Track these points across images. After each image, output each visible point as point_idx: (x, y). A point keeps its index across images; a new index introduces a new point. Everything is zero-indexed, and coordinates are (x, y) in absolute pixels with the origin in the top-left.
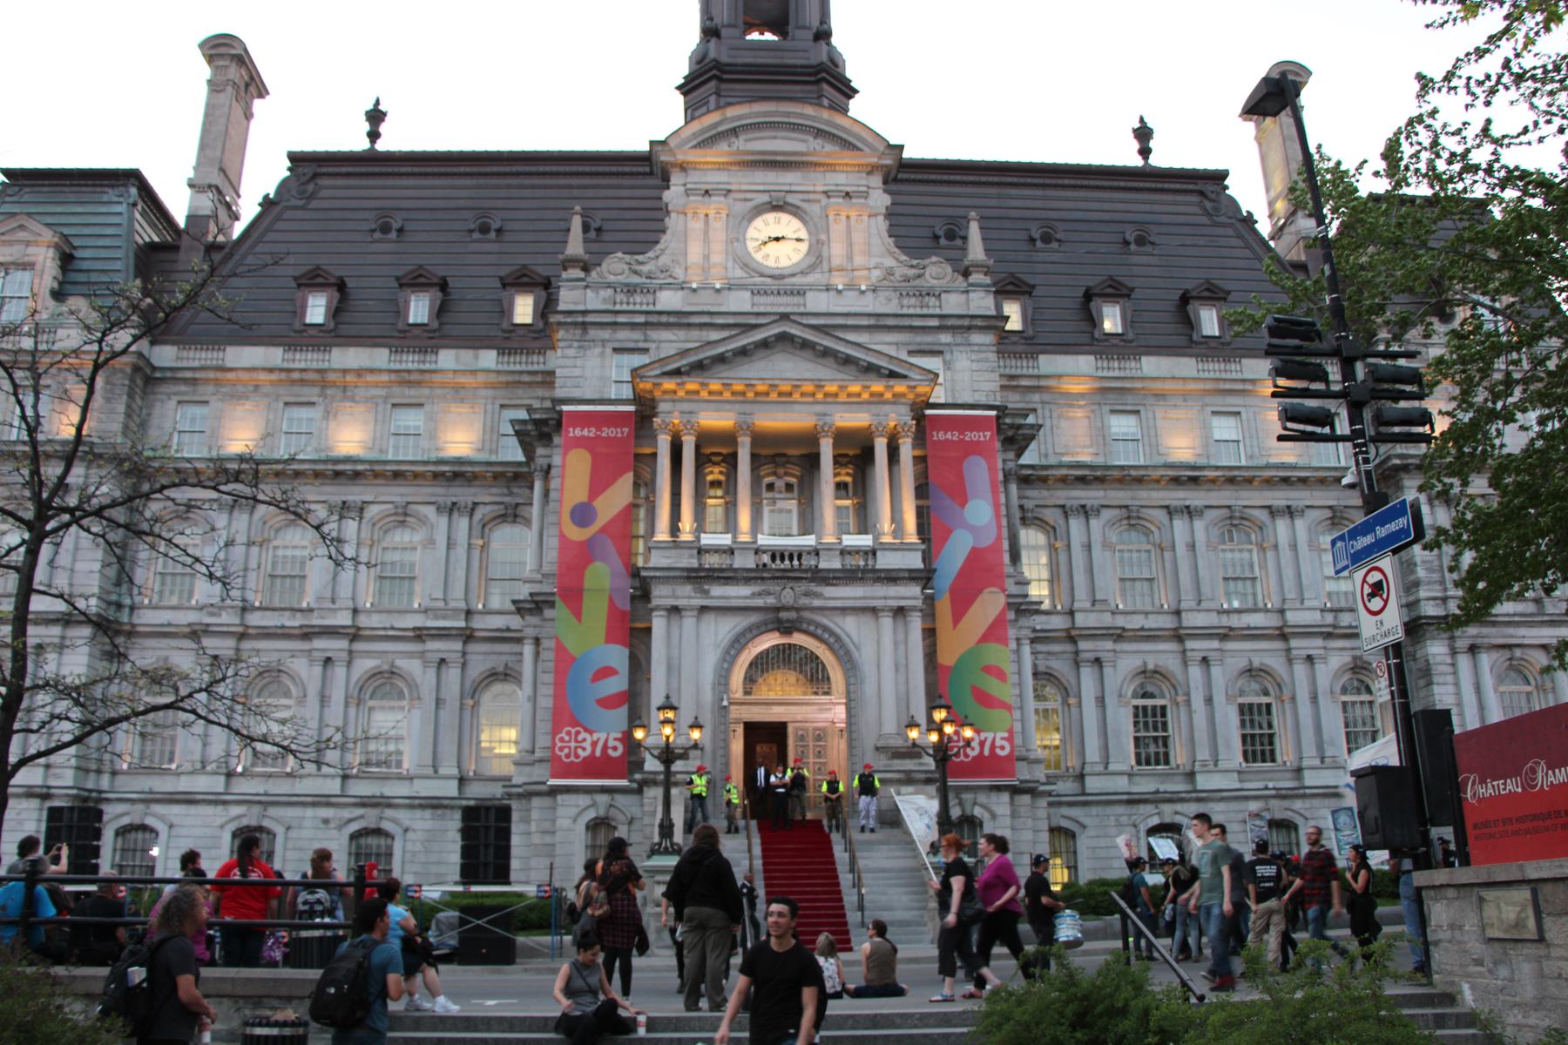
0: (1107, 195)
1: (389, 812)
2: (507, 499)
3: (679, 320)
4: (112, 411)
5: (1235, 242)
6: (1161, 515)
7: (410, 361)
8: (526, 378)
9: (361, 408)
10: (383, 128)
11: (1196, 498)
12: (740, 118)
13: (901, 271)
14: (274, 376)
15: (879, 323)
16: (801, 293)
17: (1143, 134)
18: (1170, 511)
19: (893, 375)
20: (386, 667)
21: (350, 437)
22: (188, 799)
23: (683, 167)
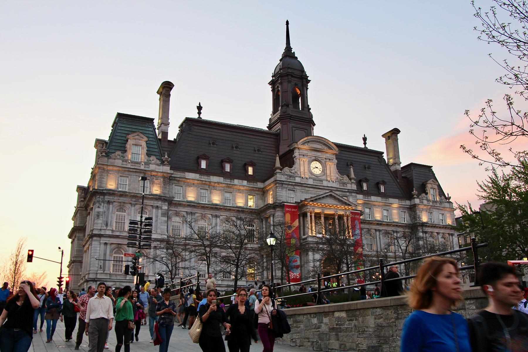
0: (361, 155)
3: (301, 185)
4: (166, 188)
5: (385, 170)
6: (374, 231)
7: (228, 181)
9: (218, 192)
10: (202, 111)
11: (381, 228)
13: (339, 177)
14: (199, 182)
15: (337, 189)
16: (322, 181)
17: (365, 139)
18: (376, 230)
19: (349, 205)
21: (216, 199)
23: (299, 148)
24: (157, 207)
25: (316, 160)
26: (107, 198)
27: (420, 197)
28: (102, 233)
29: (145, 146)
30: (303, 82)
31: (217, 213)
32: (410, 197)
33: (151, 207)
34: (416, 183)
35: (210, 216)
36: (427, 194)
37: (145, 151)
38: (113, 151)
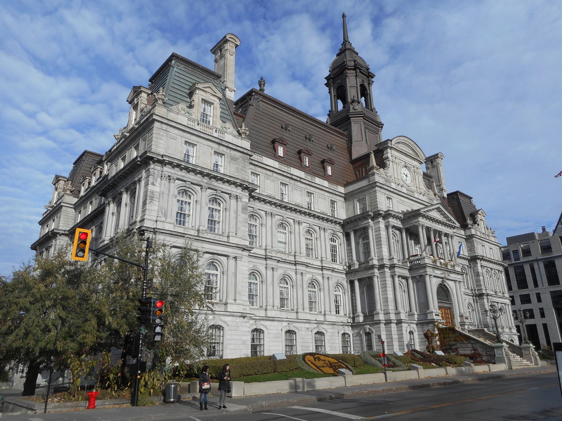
1: (322, 326)
2: (334, 229)
7: (309, 178)
8: (337, 193)
12: (401, 140)
20: (314, 278)
22: (272, 319)
24: (237, 197)
25: (406, 167)
26: (168, 170)
27: (474, 227)
28: (160, 226)
29: (218, 106)
30: (369, 80)
31: (301, 218)
32: (464, 226)
33: (227, 196)
34: (467, 212)
35: (291, 221)
36: (478, 225)
37: (219, 114)
38: (172, 103)
